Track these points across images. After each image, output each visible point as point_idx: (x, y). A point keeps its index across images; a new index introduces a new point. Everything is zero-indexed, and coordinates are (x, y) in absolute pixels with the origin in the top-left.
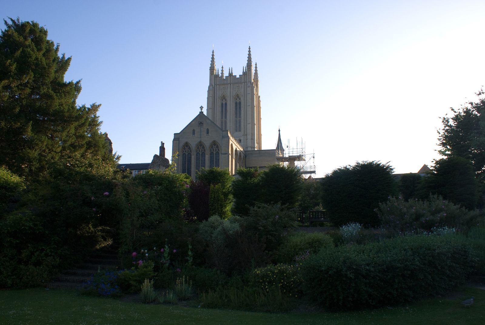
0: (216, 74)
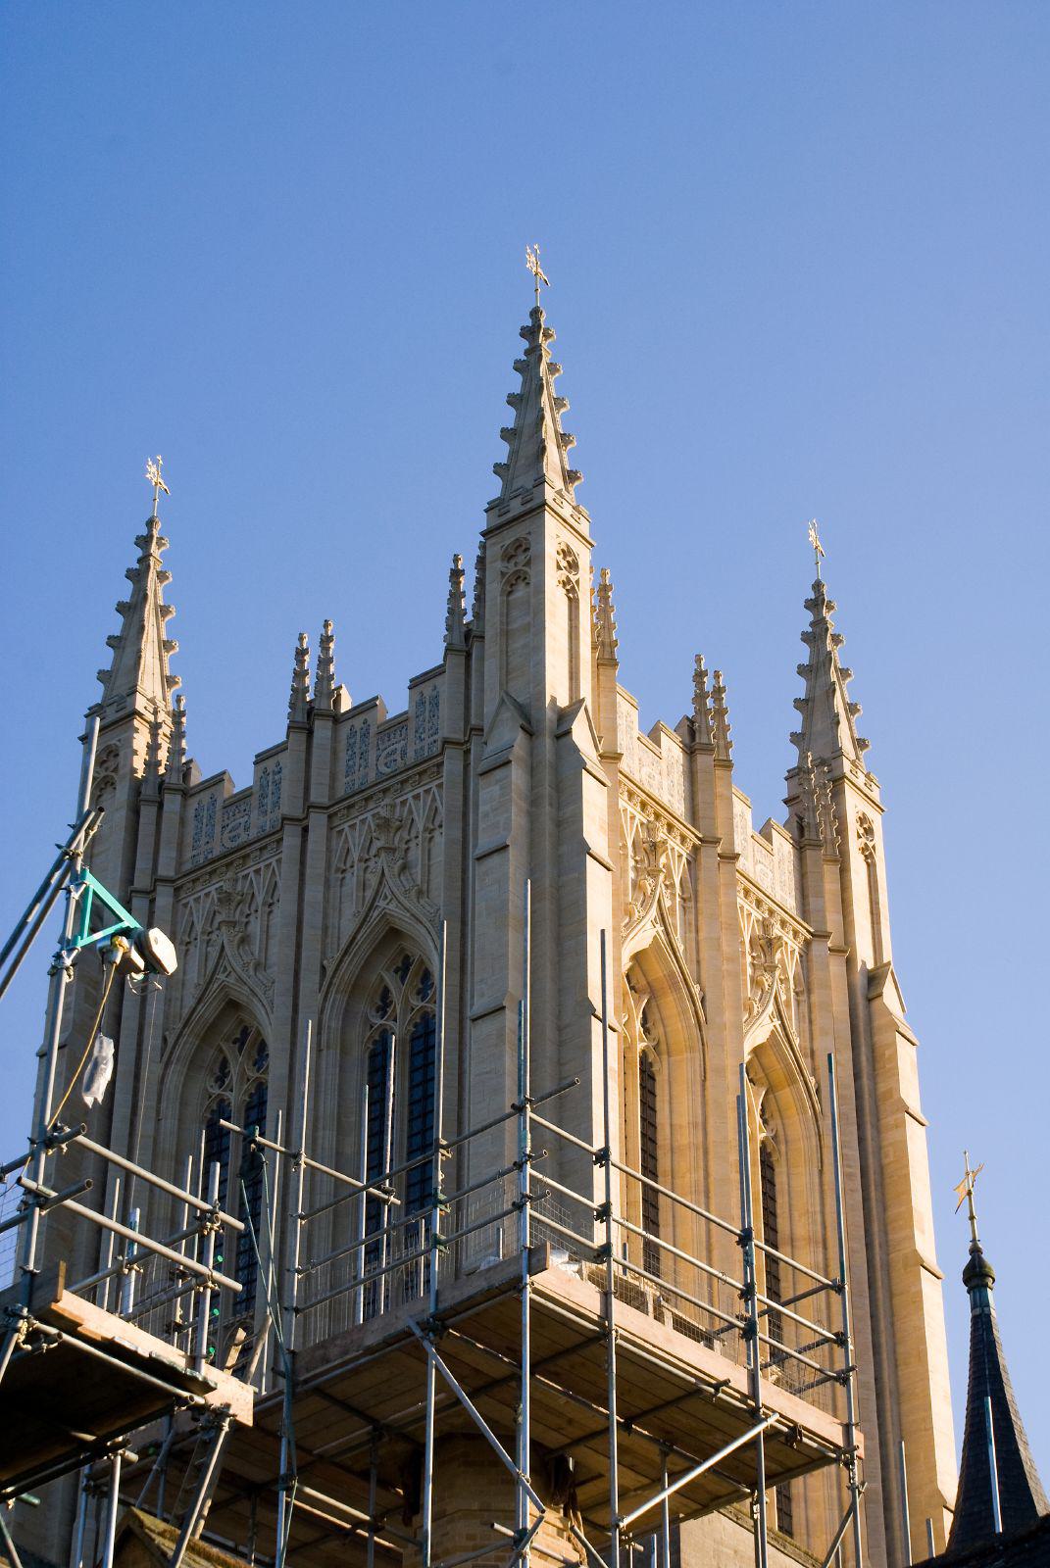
0: (152, 764)
